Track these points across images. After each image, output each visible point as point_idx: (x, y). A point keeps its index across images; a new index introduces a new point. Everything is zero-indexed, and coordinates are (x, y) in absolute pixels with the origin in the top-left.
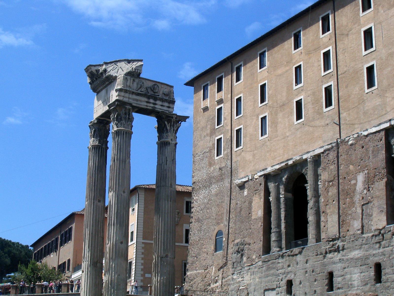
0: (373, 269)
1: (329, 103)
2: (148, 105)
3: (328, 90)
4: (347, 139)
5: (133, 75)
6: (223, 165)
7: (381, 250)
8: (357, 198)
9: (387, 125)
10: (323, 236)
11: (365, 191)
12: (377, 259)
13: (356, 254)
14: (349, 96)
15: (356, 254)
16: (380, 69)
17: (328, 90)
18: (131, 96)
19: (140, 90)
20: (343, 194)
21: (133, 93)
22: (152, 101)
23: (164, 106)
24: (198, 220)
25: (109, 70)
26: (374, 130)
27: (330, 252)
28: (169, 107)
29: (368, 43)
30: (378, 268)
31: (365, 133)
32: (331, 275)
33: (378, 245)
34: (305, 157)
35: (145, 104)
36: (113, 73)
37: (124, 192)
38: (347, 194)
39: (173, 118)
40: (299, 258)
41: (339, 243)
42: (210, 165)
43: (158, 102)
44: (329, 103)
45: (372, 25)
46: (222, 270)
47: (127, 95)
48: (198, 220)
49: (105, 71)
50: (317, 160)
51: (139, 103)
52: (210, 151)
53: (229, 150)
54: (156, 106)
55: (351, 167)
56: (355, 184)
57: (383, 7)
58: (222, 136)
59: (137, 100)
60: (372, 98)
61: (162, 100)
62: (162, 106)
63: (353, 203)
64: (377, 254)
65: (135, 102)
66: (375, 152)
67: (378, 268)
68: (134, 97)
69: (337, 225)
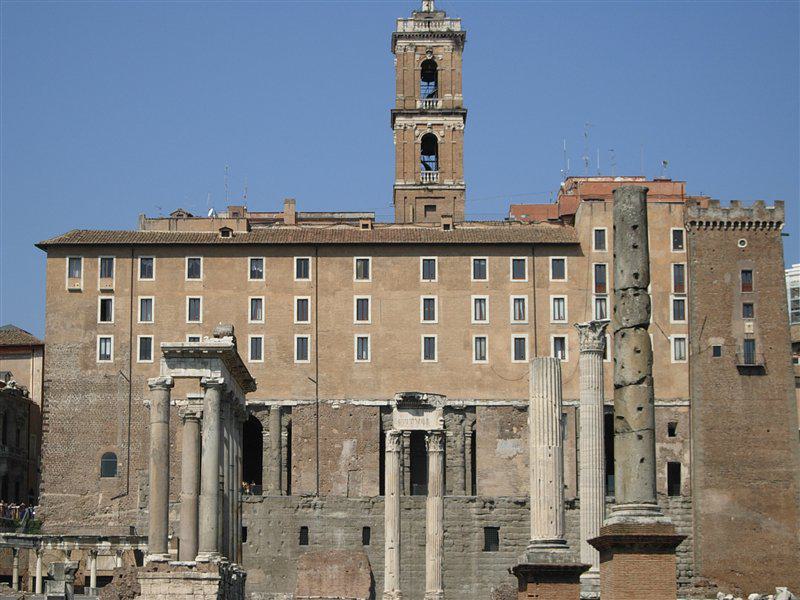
0: (361, 531)
1: (302, 355)
3: (302, 342)
4: (329, 402)
6: (113, 373)
7: (370, 516)
8: (342, 463)
9: (385, 403)
10: (293, 490)
11: (353, 459)
12: (366, 524)
13: (340, 515)
14: (332, 358)
15: (340, 515)
16: (373, 345)
17: (302, 342)
20: (324, 456)
24: (62, 431)
25: (430, 399)
26: (368, 403)
27: (303, 507)
29: (362, 313)
30: (366, 530)
31: (357, 403)
32: (304, 530)
33: (367, 511)
34: (267, 404)
36: (433, 404)
38: (328, 455)
40: (258, 506)
41: (315, 500)
42: (86, 367)
44: (302, 355)
45: (369, 297)
46: (118, 500)
48: (62, 431)
49: (426, 401)
50: (285, 410)
52: (85, 348)
53: (126, 358)
55: (335, 431)
56: (341, 449)
57: (384, 284)
58: (112, 336)
60: (362, 368)
63: (335, 467)
64: (366, 518)
66: (367, 425)
67: (366, 530)
69: (315, 484)
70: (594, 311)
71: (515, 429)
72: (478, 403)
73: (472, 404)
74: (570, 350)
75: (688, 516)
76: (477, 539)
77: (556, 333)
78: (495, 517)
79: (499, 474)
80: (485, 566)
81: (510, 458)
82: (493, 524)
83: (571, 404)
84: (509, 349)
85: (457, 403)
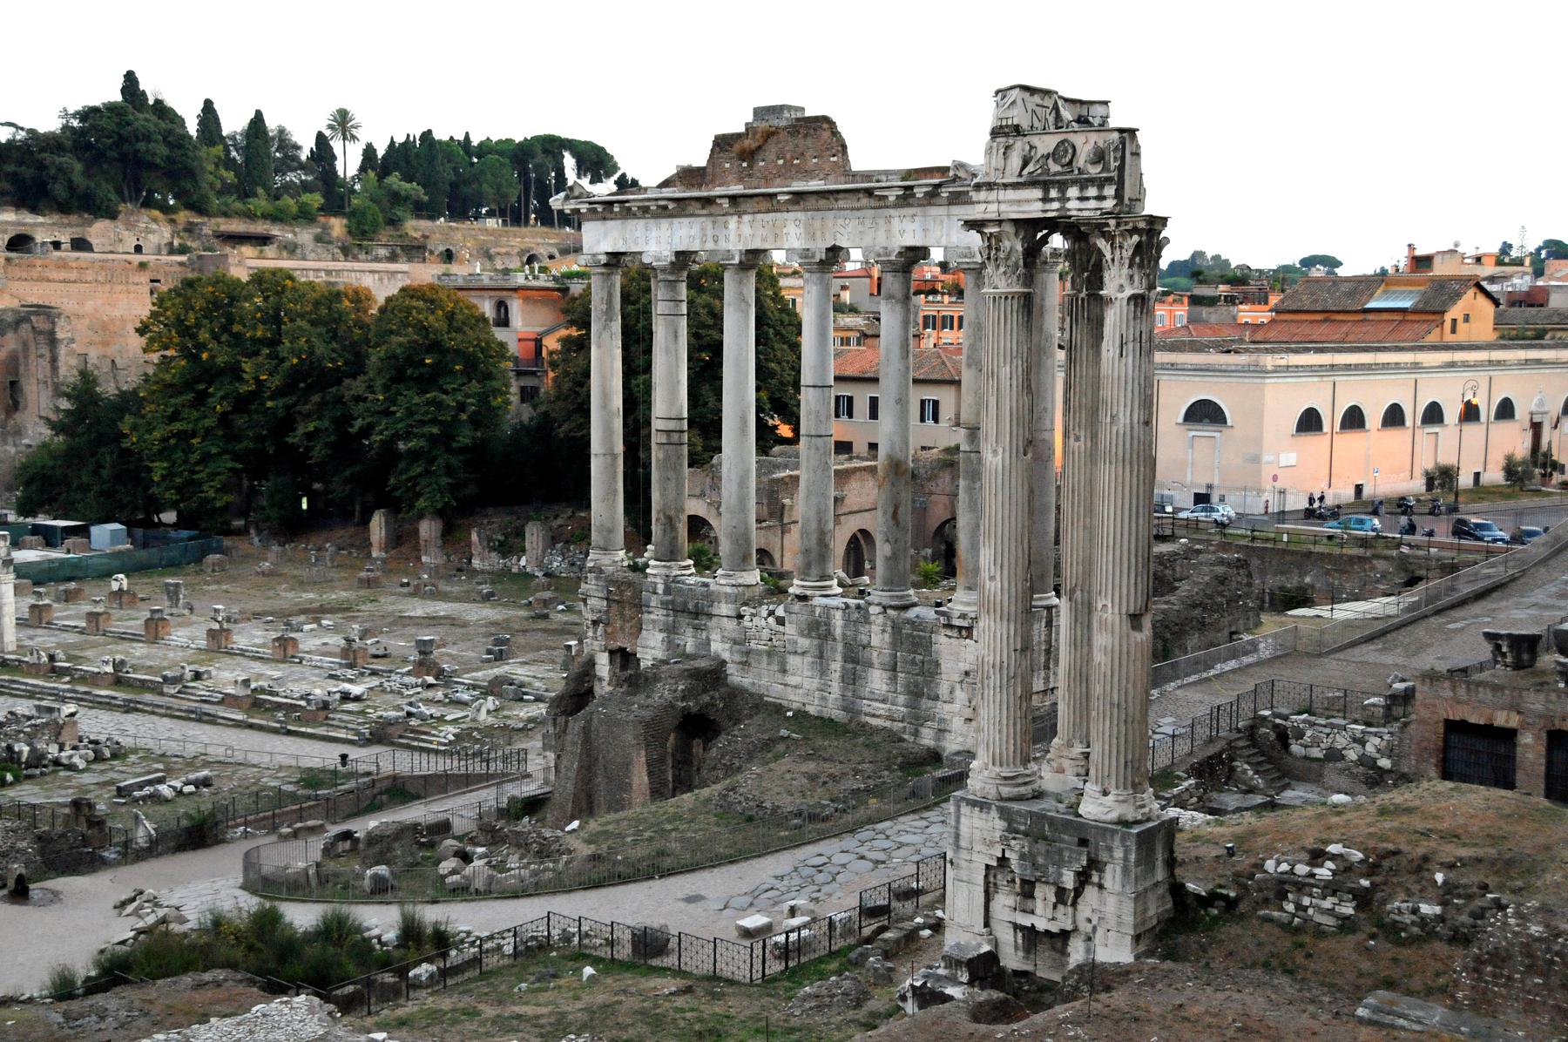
2: (1048, 206)
5: (1007, 135)
18: (1002, 192)
19: (1025, 172)
21: (1005, 186)
22: (1053, 193)
23: (1088, 199)
28: (1100, 198)
35: (1039, 205)
37: (995, 452)
39: (1107, 225)
43: (1073, 192)
47: (993, 195)
51: (1025, 208)
54: (1070, 205)
59: (1019, 202)
61: (1083, 184)
62: (1081, 199)
65: (1015, 208)
68: (1011, 194)
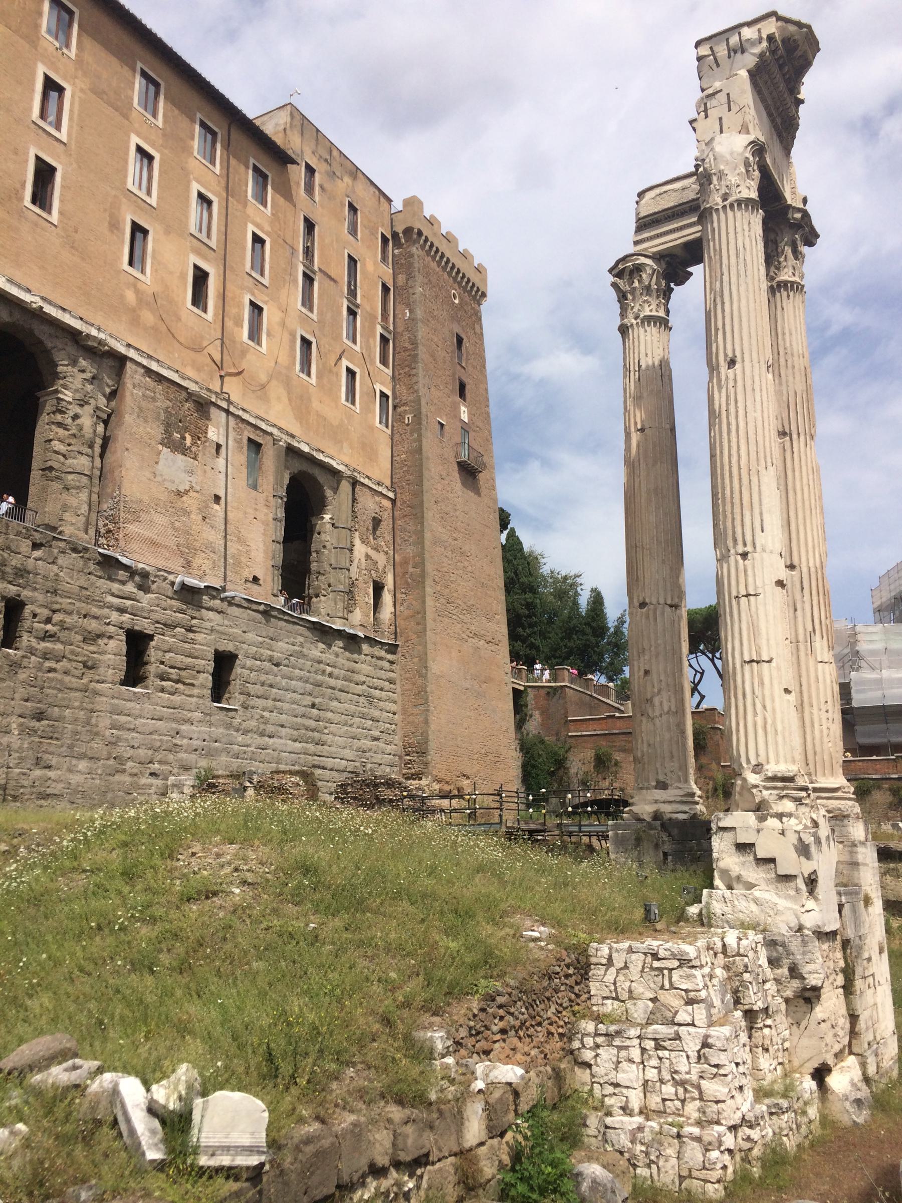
70: (300, 289)
71: (188, 441)
72: (132, 354)
73: (122, 350)
74: (268, 334)
75: (392, 675)
76: (113, 653)
77: (253, 294)
78: (151, 609)
79: (161, 520)
80: (123, 719)
81: (179, 494)
82: (144, 625)
83: (269, 429)
84: (183, 276)
85: (94, 332)
